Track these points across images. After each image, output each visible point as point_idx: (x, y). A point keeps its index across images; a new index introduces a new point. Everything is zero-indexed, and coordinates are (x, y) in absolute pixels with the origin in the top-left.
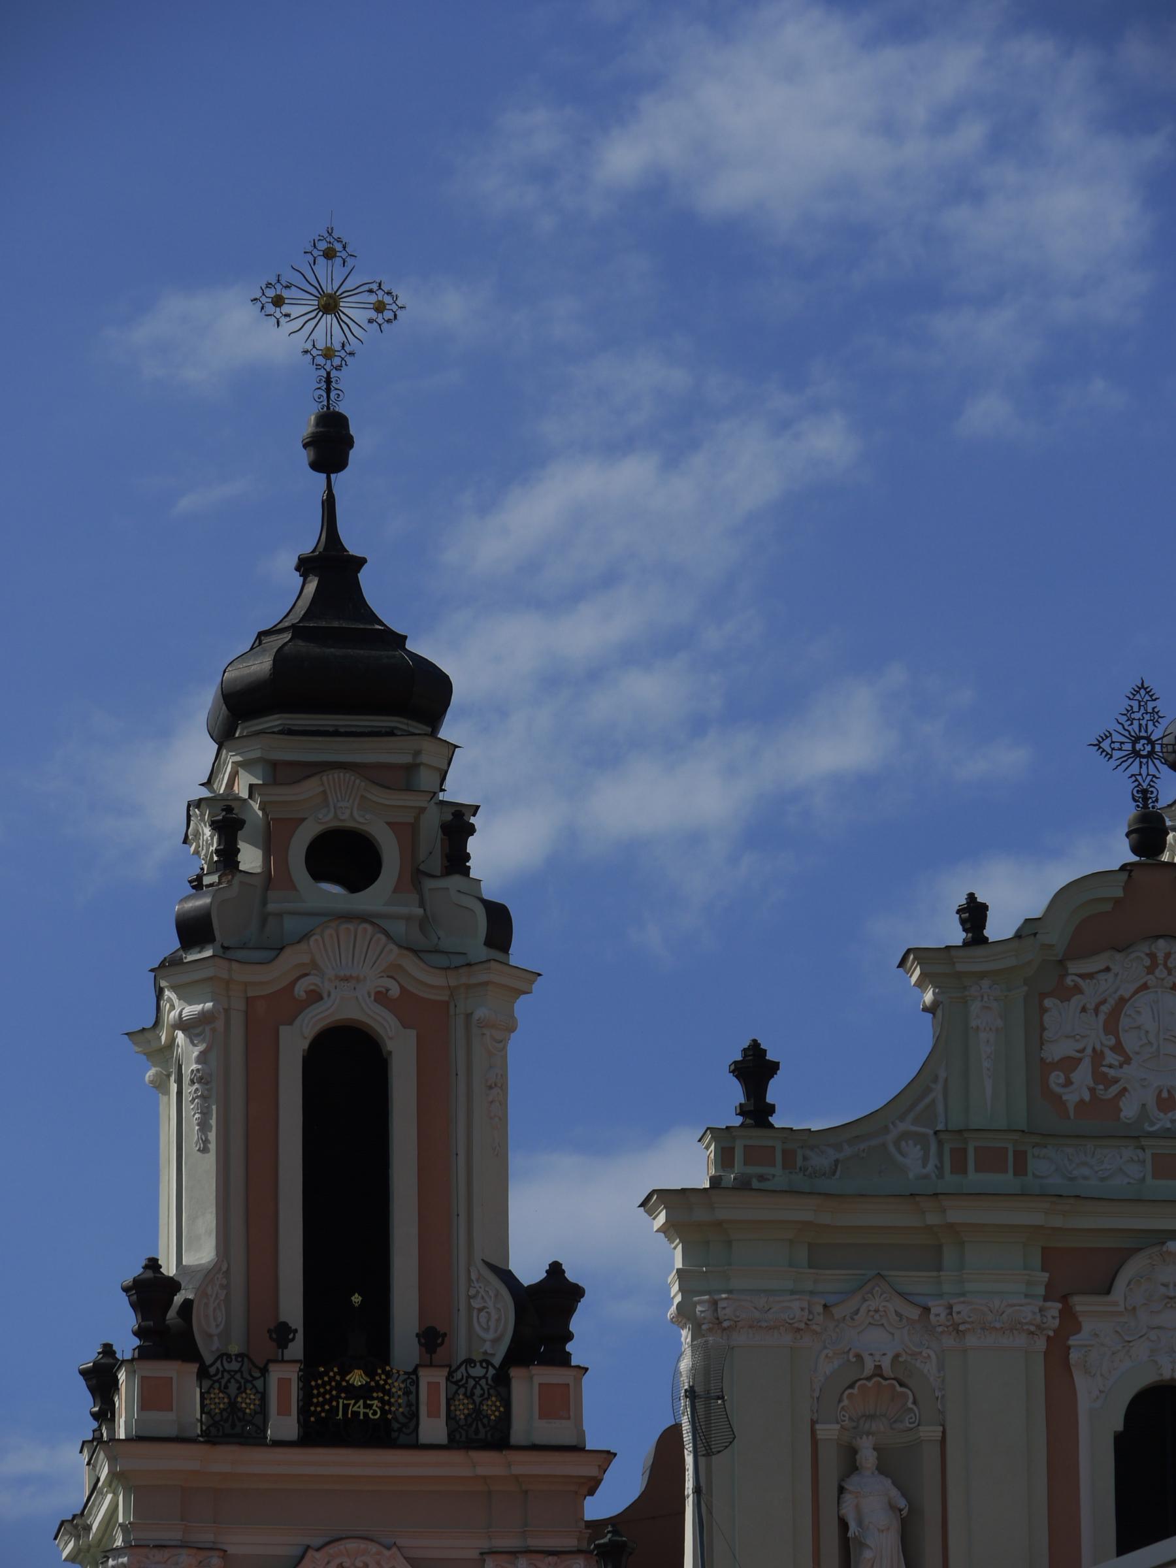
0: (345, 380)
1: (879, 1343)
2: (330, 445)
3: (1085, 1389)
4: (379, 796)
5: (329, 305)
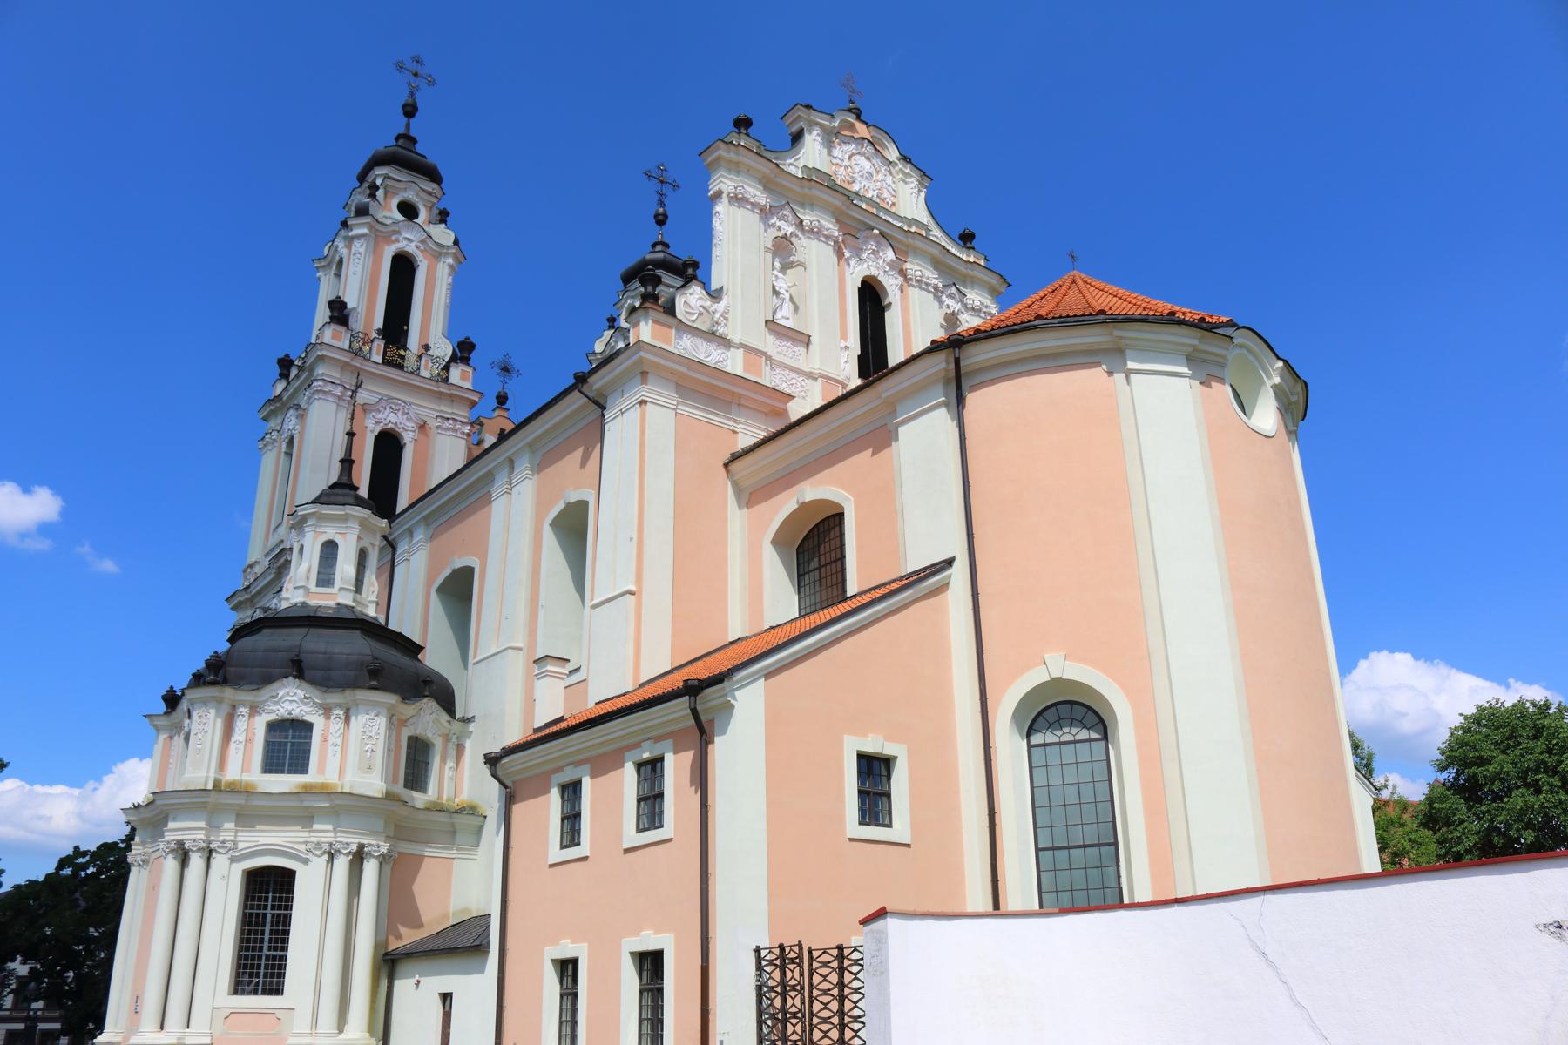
0: (418, 95)
1: (788, 229)
2: (410, 111)
3: (848, 271)
4: (422, 194)
5: (416, 75)
